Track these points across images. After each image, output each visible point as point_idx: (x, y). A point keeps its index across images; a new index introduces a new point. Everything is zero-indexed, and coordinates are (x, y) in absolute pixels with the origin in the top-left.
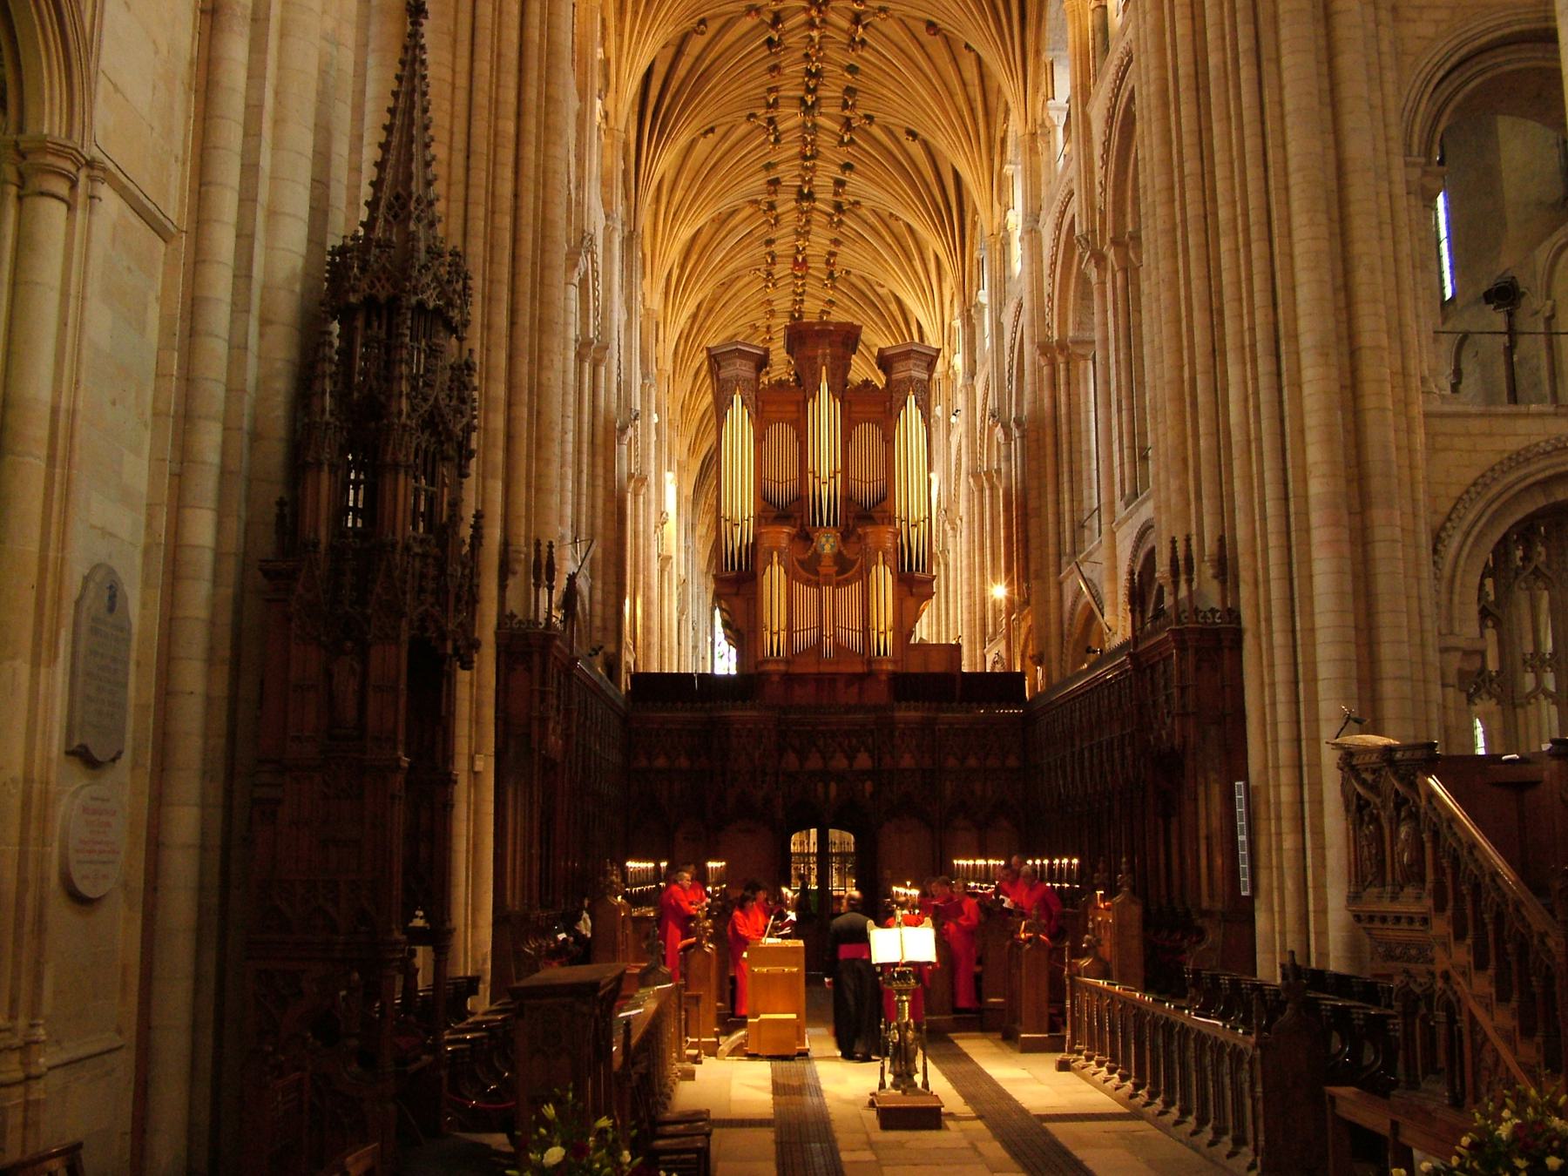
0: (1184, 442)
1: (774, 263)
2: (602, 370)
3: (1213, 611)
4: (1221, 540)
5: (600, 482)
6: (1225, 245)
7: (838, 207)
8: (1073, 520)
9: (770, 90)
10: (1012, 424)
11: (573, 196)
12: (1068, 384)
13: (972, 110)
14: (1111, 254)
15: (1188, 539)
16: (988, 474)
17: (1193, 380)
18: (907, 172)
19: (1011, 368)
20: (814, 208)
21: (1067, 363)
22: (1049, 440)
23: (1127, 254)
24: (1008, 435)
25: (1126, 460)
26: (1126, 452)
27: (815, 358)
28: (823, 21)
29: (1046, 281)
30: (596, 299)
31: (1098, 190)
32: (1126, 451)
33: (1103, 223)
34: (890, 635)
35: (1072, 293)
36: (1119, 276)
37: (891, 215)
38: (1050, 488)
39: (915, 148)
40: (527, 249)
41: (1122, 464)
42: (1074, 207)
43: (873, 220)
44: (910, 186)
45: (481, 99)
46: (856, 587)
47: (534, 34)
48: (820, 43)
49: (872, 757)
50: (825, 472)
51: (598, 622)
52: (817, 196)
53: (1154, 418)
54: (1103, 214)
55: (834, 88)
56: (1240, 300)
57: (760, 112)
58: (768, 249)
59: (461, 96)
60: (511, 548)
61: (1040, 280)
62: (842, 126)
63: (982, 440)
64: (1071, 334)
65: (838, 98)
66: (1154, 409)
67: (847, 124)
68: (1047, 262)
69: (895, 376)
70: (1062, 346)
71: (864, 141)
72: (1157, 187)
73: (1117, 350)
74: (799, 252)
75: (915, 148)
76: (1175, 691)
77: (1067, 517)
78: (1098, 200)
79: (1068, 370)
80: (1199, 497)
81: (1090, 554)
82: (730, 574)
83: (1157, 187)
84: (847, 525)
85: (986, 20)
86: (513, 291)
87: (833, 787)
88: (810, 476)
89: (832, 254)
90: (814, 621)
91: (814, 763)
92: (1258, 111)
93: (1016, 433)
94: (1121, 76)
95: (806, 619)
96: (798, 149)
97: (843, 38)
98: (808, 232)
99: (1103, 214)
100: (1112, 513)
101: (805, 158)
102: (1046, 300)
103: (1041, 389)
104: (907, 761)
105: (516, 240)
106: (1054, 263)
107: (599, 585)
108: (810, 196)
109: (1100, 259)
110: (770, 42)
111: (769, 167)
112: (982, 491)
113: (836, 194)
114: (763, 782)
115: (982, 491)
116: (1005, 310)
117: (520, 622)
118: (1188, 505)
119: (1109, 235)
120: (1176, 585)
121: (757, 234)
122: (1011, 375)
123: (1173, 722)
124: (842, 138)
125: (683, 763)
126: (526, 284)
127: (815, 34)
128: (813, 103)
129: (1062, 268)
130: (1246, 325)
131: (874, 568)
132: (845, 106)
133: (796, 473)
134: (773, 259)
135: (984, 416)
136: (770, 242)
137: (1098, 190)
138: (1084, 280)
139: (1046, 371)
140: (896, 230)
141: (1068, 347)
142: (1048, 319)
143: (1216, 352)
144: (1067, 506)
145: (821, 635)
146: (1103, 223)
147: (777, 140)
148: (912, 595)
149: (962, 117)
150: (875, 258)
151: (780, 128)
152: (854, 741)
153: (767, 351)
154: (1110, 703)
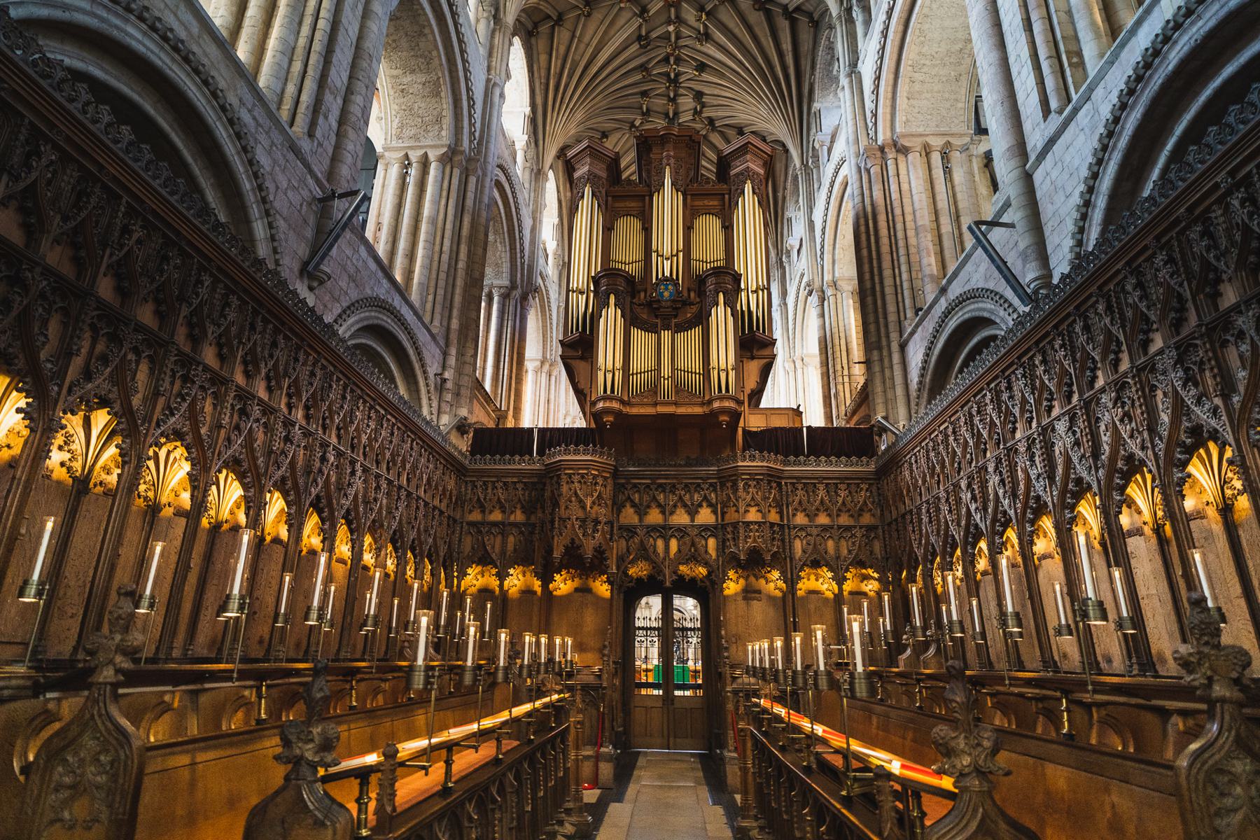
2: (473, 180)
30: (471, 125)
34: (732, 374)
46: (696, 333)
48: (676, 42)
49: (715, 512)
87: (674, 544)
88: (654, 255)
90: (652, 364)
91: (654, 517)
95: (641, 359)
102: (869, 115)
104: (753, 515)
107: (453, 351)
114: (595, 530)
125: (519, 516)
127: (671, 28)
139: (875, 170)
148: (753, 358)
152: (696, 496)
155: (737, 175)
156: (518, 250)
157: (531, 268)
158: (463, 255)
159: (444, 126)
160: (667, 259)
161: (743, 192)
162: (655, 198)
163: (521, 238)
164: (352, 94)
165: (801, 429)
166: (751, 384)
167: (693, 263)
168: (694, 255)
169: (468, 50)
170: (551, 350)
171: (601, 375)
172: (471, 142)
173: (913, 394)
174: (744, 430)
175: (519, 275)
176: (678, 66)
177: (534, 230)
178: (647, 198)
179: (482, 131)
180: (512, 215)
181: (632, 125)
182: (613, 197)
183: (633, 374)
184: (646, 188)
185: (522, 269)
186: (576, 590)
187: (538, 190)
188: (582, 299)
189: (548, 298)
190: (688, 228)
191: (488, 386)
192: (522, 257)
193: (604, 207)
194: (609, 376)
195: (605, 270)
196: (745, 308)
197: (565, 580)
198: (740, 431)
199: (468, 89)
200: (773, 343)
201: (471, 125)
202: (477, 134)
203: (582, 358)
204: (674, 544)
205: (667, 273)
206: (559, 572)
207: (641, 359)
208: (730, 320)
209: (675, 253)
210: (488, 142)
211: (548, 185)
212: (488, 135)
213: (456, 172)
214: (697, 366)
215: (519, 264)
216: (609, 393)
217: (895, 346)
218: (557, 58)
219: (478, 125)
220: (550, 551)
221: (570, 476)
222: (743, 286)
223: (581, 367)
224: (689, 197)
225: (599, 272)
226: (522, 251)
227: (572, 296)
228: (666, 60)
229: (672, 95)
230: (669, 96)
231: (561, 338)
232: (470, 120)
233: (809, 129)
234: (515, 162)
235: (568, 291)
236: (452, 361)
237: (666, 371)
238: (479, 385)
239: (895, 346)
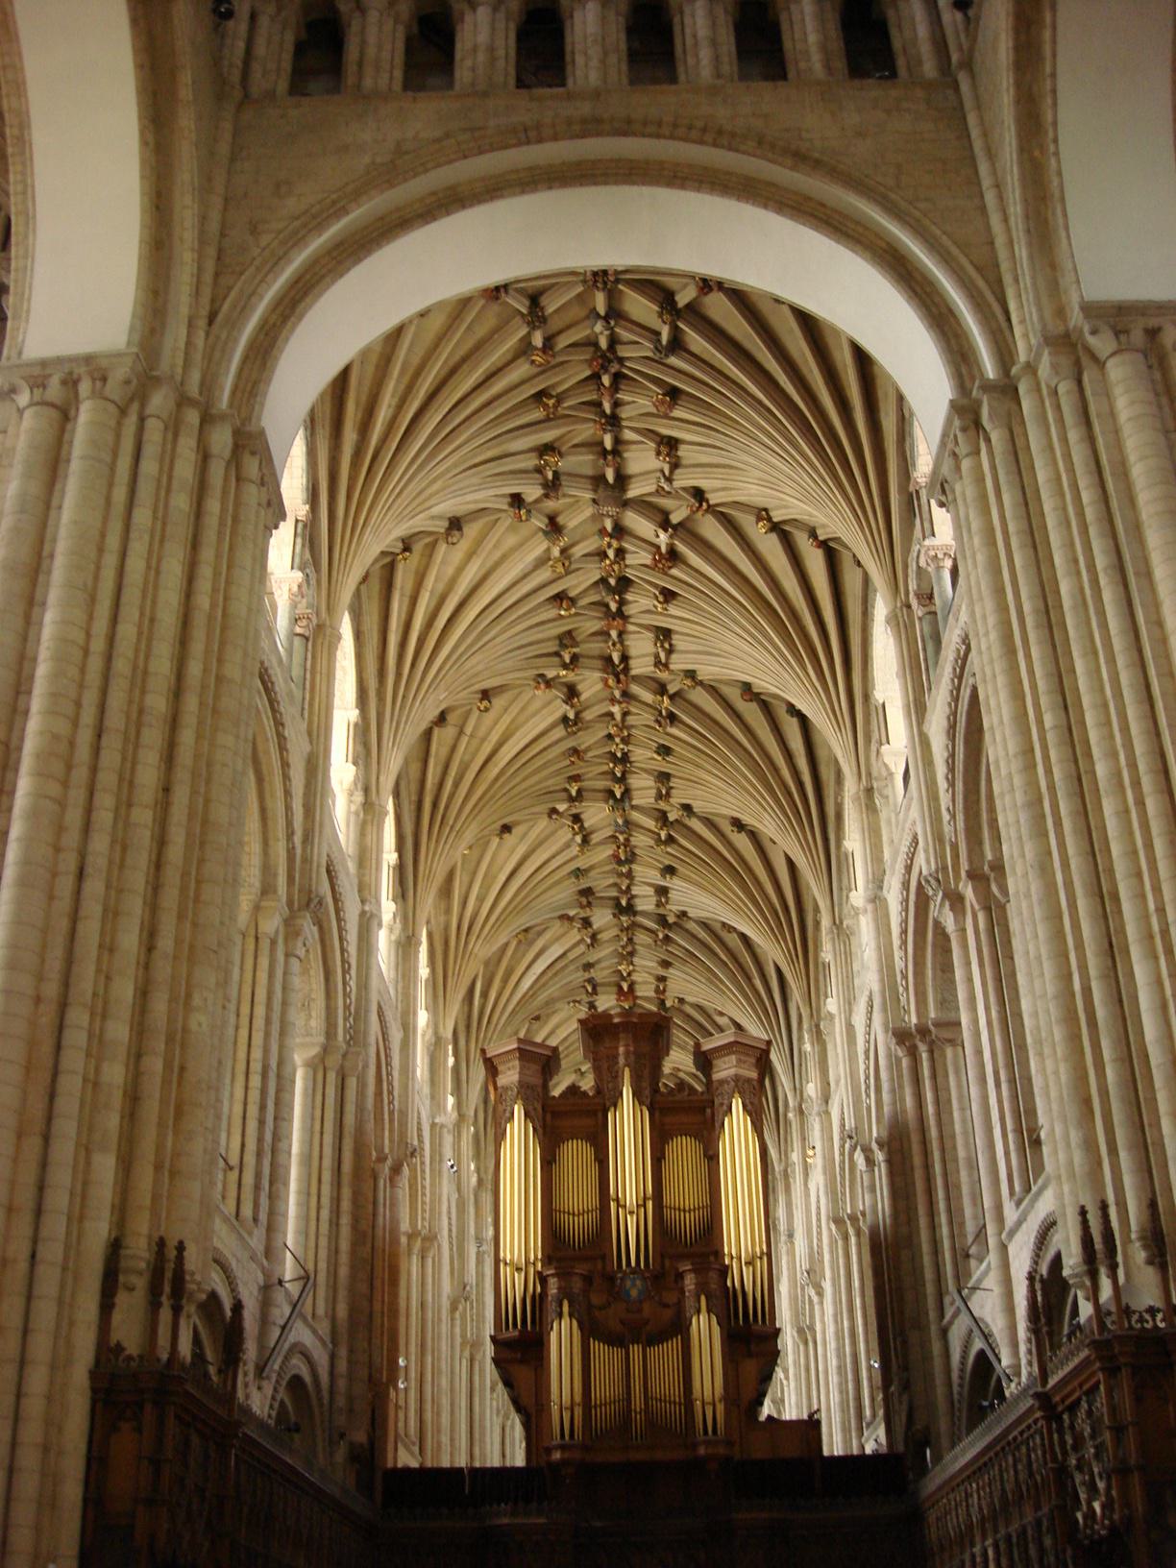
0: (1085, 1078)
1: (595, 992)
3: (1152, 1311)
4: (1153, 1205)
5: (345, 1220)
6: (1109, 807)
7: (662, 920)
8: (953, 1248)
9: (576, 778)
10: (875, 1146)
11: (299, 851)
12: (934, 1076)
14: (968, 892)
15: (1104, 1207)
16: (853, 1218)
17: (1087, 991)
18: (737, 871)
19: (867, 1077)
20: (635, 925)
21: (931, 1052)
22: (916, 1148)
23: (989, 886)
24: (870, 1162)
25: (1012, 1147)
26: (1010, 1136)
27: (616, 1057)
28: (625, 694)
29: (897, 954)
31: (946, 817)
32: (1010, 1136)
33: (956, 856)
34: (720, 1407)
35: (929, 965)
36: (981, 916)
37: (724, 924)
38: (922, 1210)
39: (742, 841)
40: (175, 852)
41: (1007, 1153)
42: (920, 859)
43: (702, 934)
44: (744, 892)
45: (121, 665)
46: (671, 1348)
47: (203, 601)
48: (623, 720)
50: (631, 1198)
51: (341, 1401)
52: (639, 908)
53: (1040, 1054)
54: (955, 847)
55: (645, 775)
56: (1139, 875)
57: (562, 807)
58: (587, 976)
59: (95, 664)
60: (123, 1252)
61: (890, 956)
62: (657, 820)
63: (843, 1177)
64: (932, 1015)
65: (650, 788)
66: (1039, 1042)
67: (662, 817)
68: (895, 930)
69: (716, 1076)
70: (923, 1031)
71: (685, 837)
72: (1011, 753)
73: (987, 1008)
74: (623, 979)
75: (742, 841)
76: (1107, 1436)
77: (946, 1244)
78: (947, 829)
79: (932, 1060)
80: (1113, 1150)
81: (980, 1281)
82: (513, 1333)
83: (1011, 753)
84: (663, 1266)
85: (804, 669)
86: (153, 907)
88: (613, 1205)
89: (662, 979)
90: (619, 1390)
92: (1132, 634)
93: (880, 1156)
94: (959, 676)
95: (605, 1387)
96: (611, 852)
97: (648, 718)
98: (632, 954)
99: (955, 847)
100: (1000, 1219)
101: (620, 862)
103: (901, 1087)
105: (161, 842)
106: (904, 932)
107: (343, 1352)
108: (630, 910)
109: (956, 900)
110: (565, 719)
111: (578, 873)
112: (846, 1238)
113: (659, 905)
115: (846, 1238)
116: (855, 1008)
117: (130, 1358)
118: (1100, 1164)
119: (964, 866)
120: (1093, 1275)
121: (571, 956)
122: (868, 1087)
123: (1109, 1488)
124: (659, 835)
126: (170, 898)
128: (623, 794)
130: (1152, 906)
131: (694, 1320)
133: (594, 1201)
134: (594, 988)
135: (842, 1139)
136: (588, 966)
137: (946, 817)
138: (939, 928)
139: (905, 1062)
140: (731, 944)
141: (930, 1031)
143: (1113, 950)
144: (945, 1231)
146: (956, 856)
147: (585, 841)
148: (750, 1355)
149: (789, 794)
150: (708, 979)
151: (586, 825)
154: (1016, 1479)
157: (403, 1113)
158: (346, 1205)
159: (314, 1014)
164: (280, 1140)
168: (667, 1200)
170: (424, 1211)
173: (957, 1405)
175: (387, 1142)
178: (600, 1115)
181: (554, 811)
185: (391, 1121)
187: (317, 638)
188: (519, 1278)
190: (658, 1159)
192: (391, 1102)
193: (540, 1131)
201: (346, 995)
207: (602, 1390)
208: (716, 1330)
209: (641, 1202)
214: (676, 1392)
215: (386, 1116)
216: (567, 1437)
217: (934, 1328)
223: (523, 1374)
224: (657, 1114)
226: (390, 1093)
228: (610, 737)
229: (619, 775)
230: (614, 774)
237: (638, 1402)
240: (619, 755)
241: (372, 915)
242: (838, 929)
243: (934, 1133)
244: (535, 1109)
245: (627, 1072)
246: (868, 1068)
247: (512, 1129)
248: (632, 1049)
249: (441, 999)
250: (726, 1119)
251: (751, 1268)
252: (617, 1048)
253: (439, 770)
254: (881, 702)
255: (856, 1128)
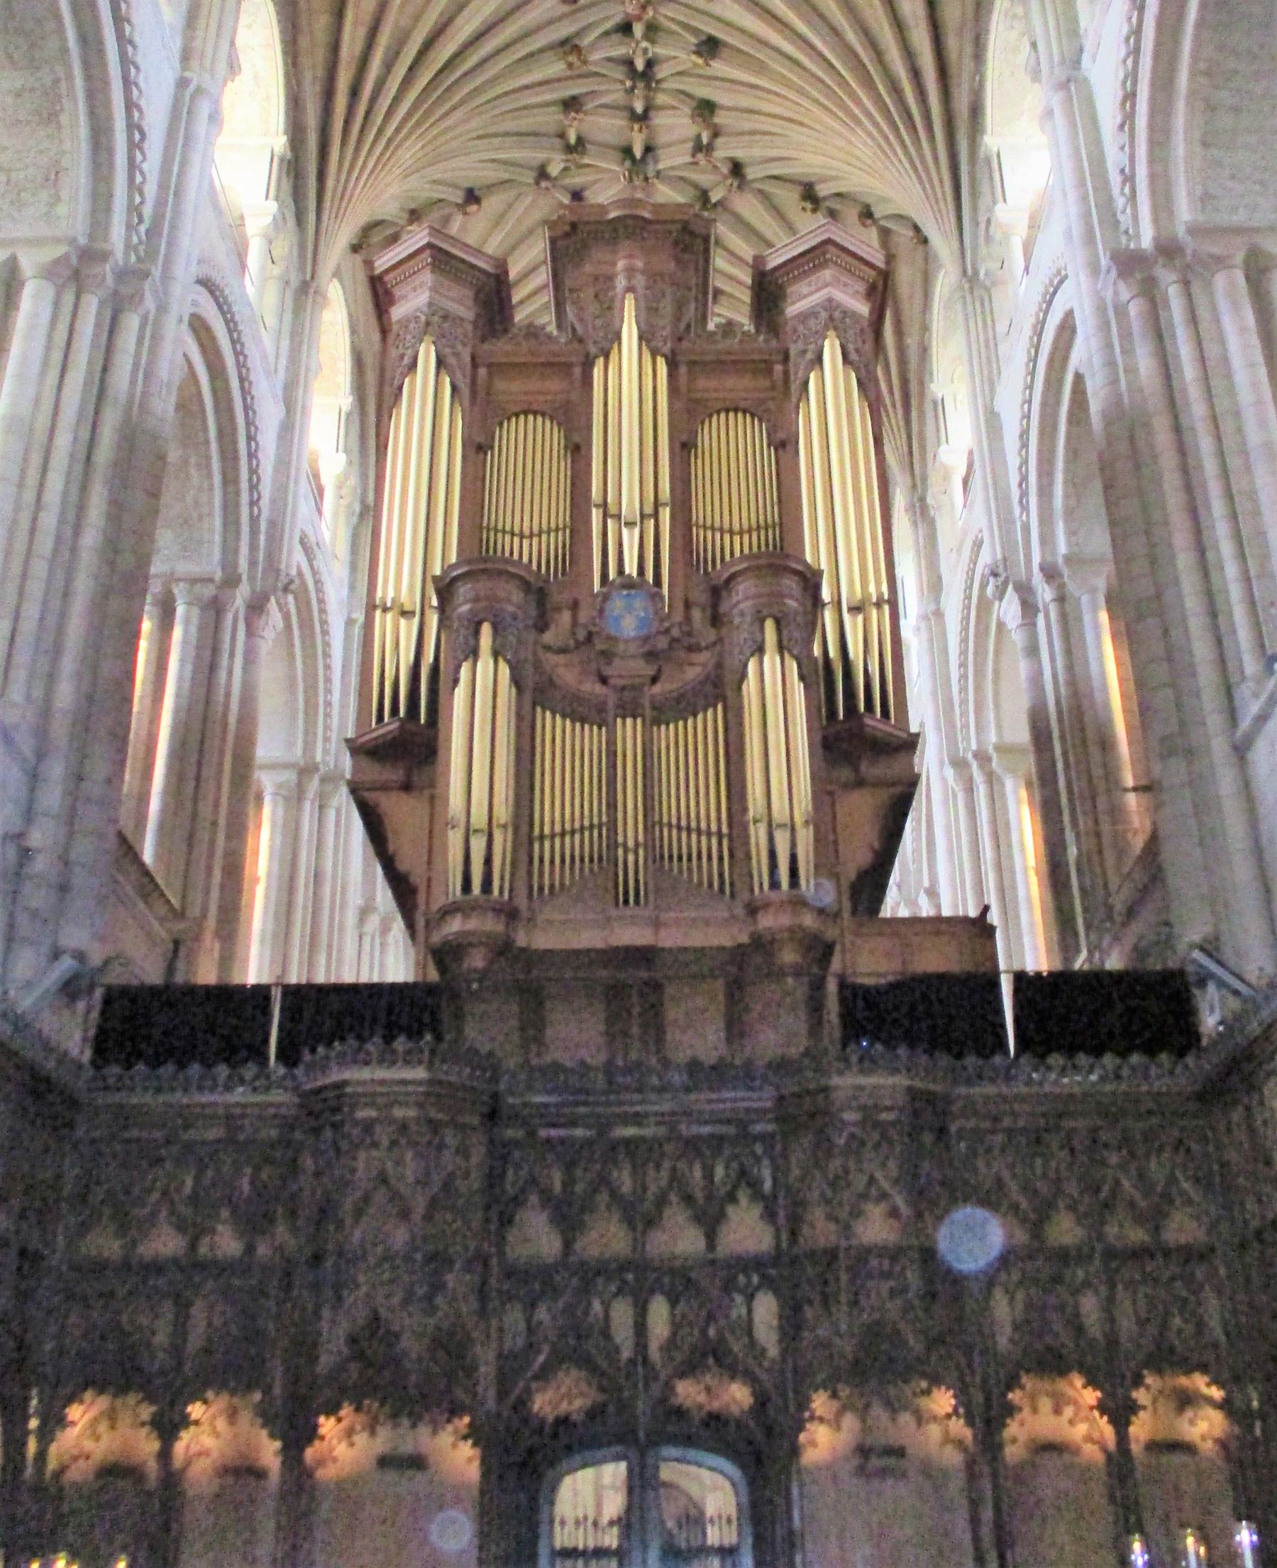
2: (131, 322)
13: (916, 74)
19: (1024, 479)
21: (1186, 284)
30: (134, 187)
34: (805, 838)
50: (630, 503)
77: (1235, 592)
129: (1153, 84)
132: (698, 147)
133: (562, 514)
142: (1125, 220)
144: (1231, 570)
145: (613, 845)
148: (860, 783)
153: (502, 266)
155: (804, 317)
156: (244, 486)
157: (276, 527)
160: (630, 524)
161: (819, 359)
162: (597, 372)
163: (252, 455)
165: (993, 984)
166: (857, 856)
167: (698, 534)
168: (698, 514)
169: (134, 19)
171: (455, 839)
172: (130, 227)
174: (843, 985)
176: (653, 42)
177: (289, 429)
179: (161, 203)
180: (230, 401)
181: (542, 174)
182: (490, 366)
183: (542, 837)
184: (576, 345)
185: (254, 532)
186: (384, 1462)
188: (408, 630)
189: (321, 601)
191: (148, 856)
192: (253, 503)
193: (465, 391)
194: (478, 845)
195: (469, 562)
196: (833, 652)
197: (350, 1433)
198: (832, 986)
199: (130, 105)
200: (910, 744)
201: (134, 187)
202: (147, 211)
203: (407, 787)
204: (659, 1314)
205: (631, 568)
206: (332, 1409)
208: (798, 690)
209: (649, 509)
210: (173, 227)
211: (327, 316)
212: (177, 213)
213: (91, 304)
218: (355, 23)
219: (151, 189)
220: (306, 1347)
221: (368, 1126)
222: (826, 595)
225: (452, 567)
226: (253, 487)
227: (384, 623)
228: (625, 28)
229: (639, 107)
231: (350, 734)
232: (131, 179)
233: (975, 195)
234: (243, 267)
235: (371, 607)
236: (52, 797)
237: (631, 830)
238: (128, 850)
239: (1219, 747)
240: (640, 65)
241: (199, 91)
242: (970, 281)
243: (1198, 409)
244: (457, 355)
245: (629, 305)
246: (1025, 462)
247: (412, 384)
248: (639, 264)
249: (311, 217)
250: (812, 376)
251: (860, 618)
252: (615, 264)
253: (362, 32)
254: (995, 150)
255: (1005, 559)
